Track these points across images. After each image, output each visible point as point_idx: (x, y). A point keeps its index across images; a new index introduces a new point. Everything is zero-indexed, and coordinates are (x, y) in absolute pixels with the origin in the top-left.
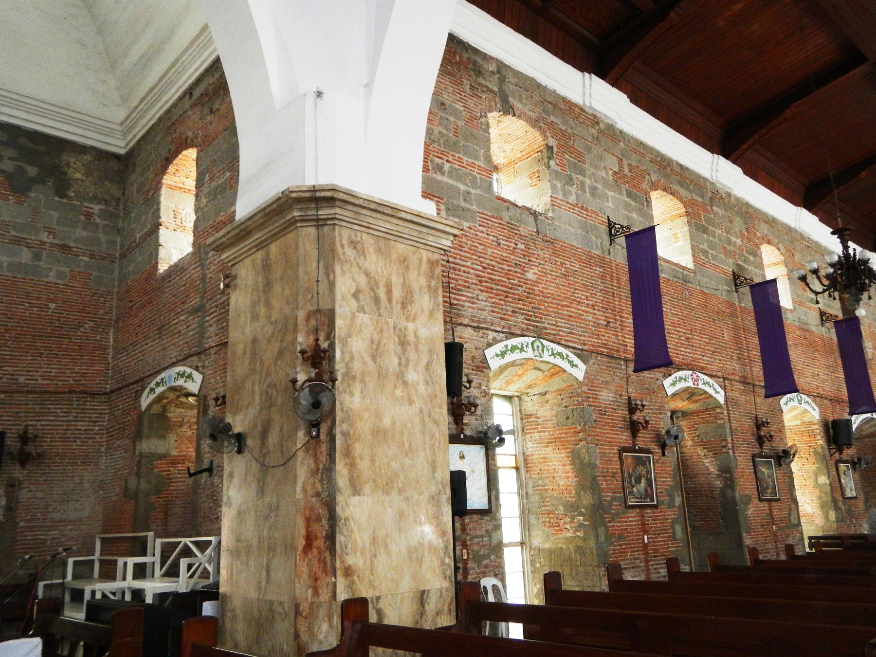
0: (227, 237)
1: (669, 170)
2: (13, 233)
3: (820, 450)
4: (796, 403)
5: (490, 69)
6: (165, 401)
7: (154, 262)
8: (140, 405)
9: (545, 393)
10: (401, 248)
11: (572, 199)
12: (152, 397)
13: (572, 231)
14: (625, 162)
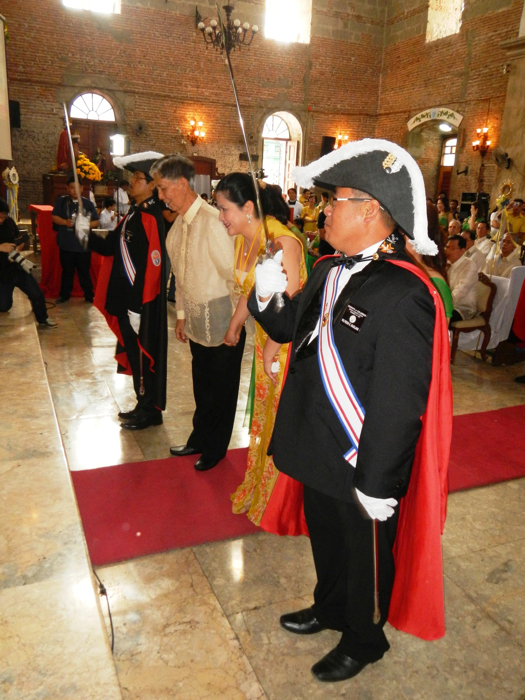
0: (516, 43)
2: (335, 9)
6: (425, 126)
7: (422, 33)
8: (407, 127)
12: (417, 123)
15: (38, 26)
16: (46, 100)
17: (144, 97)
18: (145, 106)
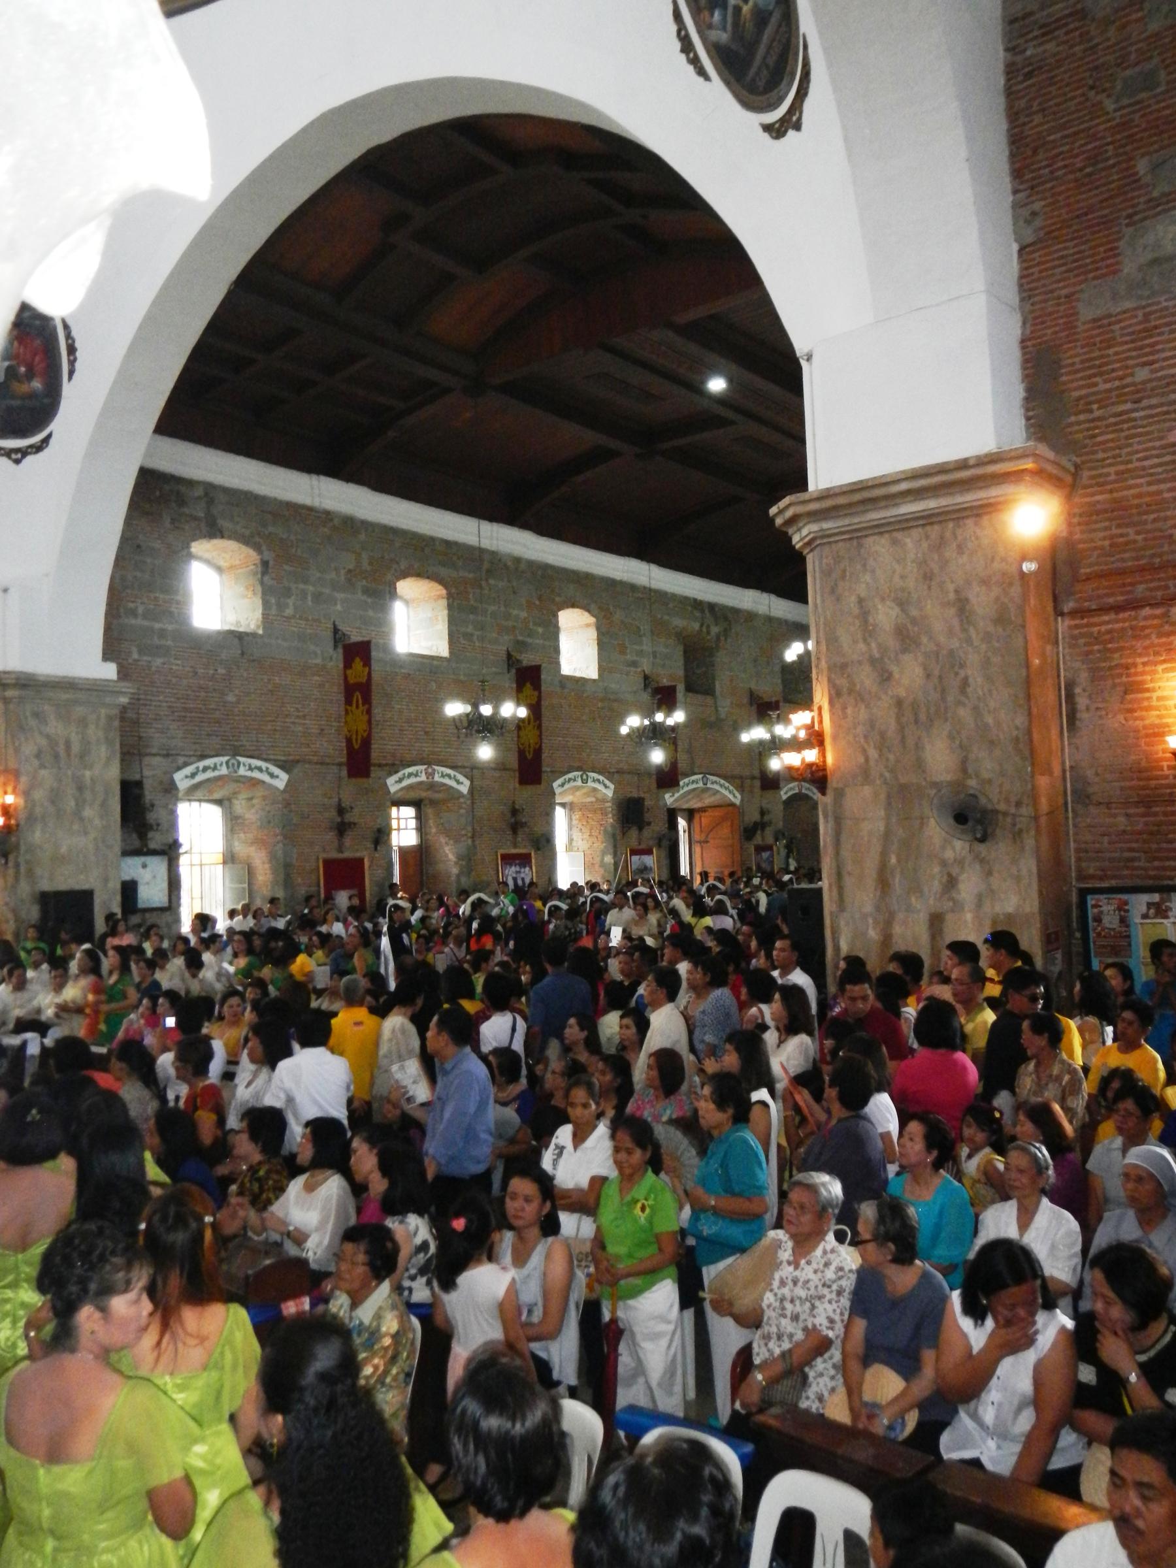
1: (427, 550)
3: (609, 829)
4: (579, 783)
5: (196, 494)
9: (251, 799)
10: (80, 710)
11: (289, 611)
13: (285, 644)
14: (364, 555)
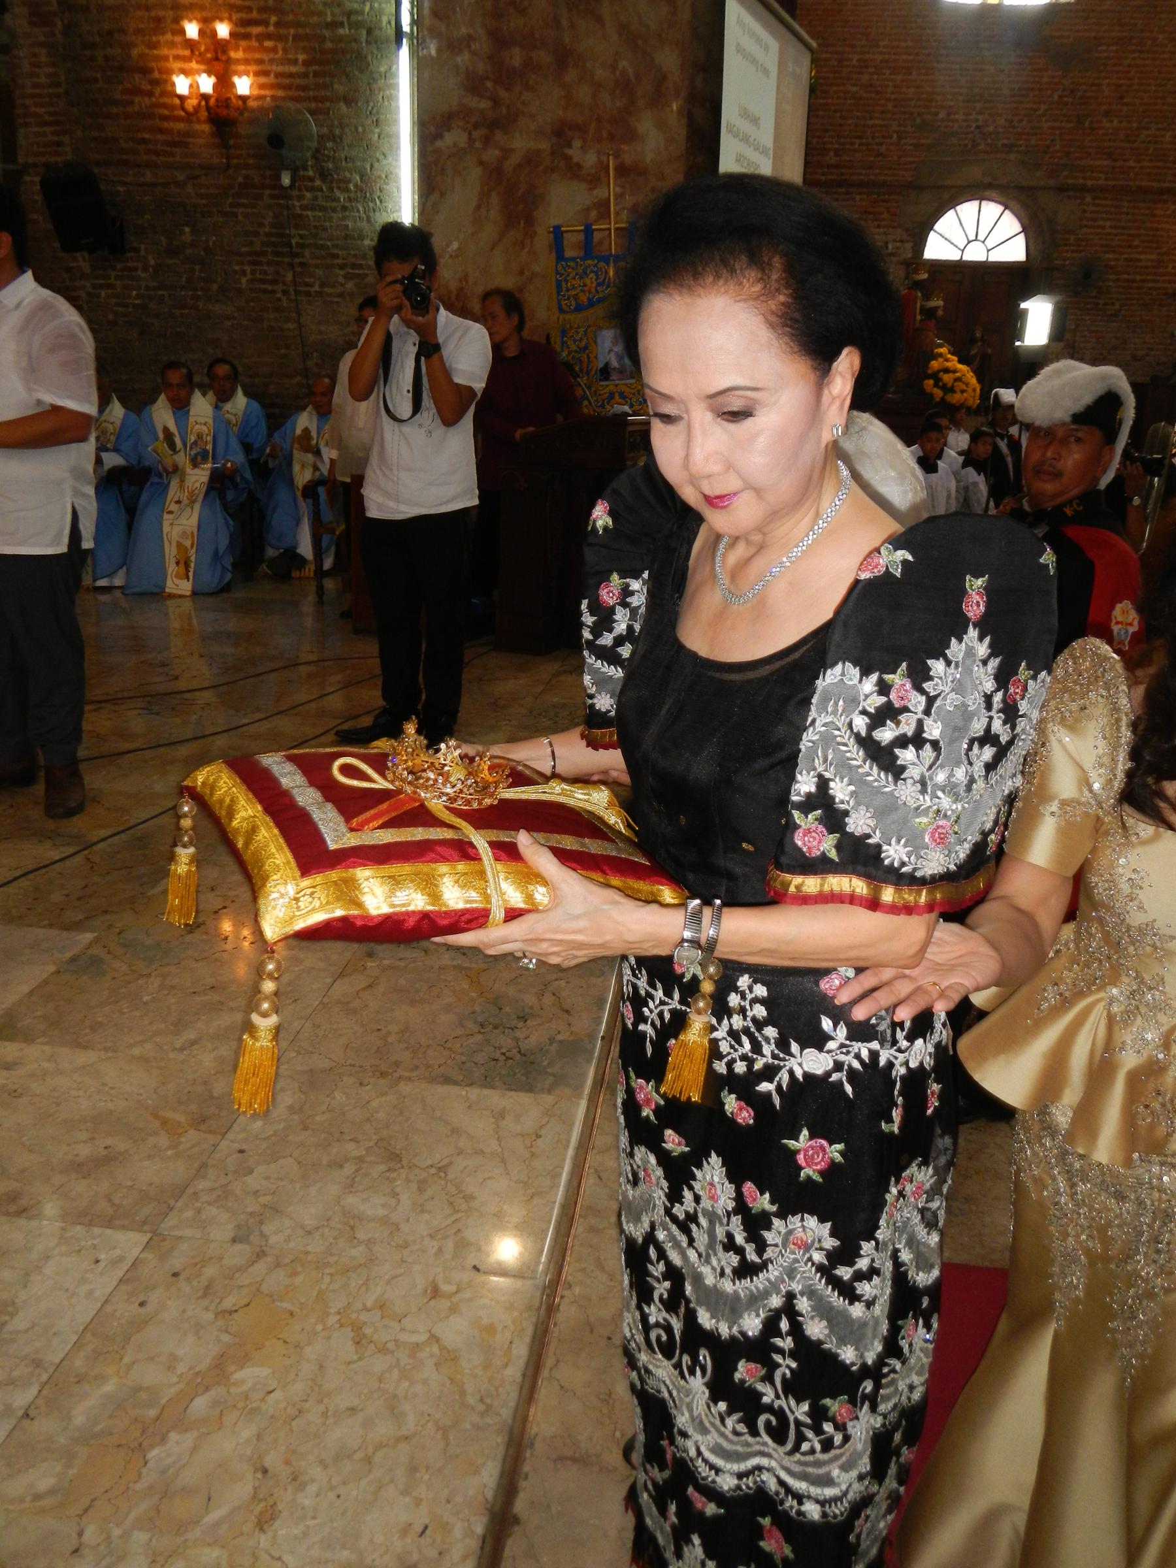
15: (879, 57)
16: (876, 223)
17: (1106, 199)
18: (1108, 219)
